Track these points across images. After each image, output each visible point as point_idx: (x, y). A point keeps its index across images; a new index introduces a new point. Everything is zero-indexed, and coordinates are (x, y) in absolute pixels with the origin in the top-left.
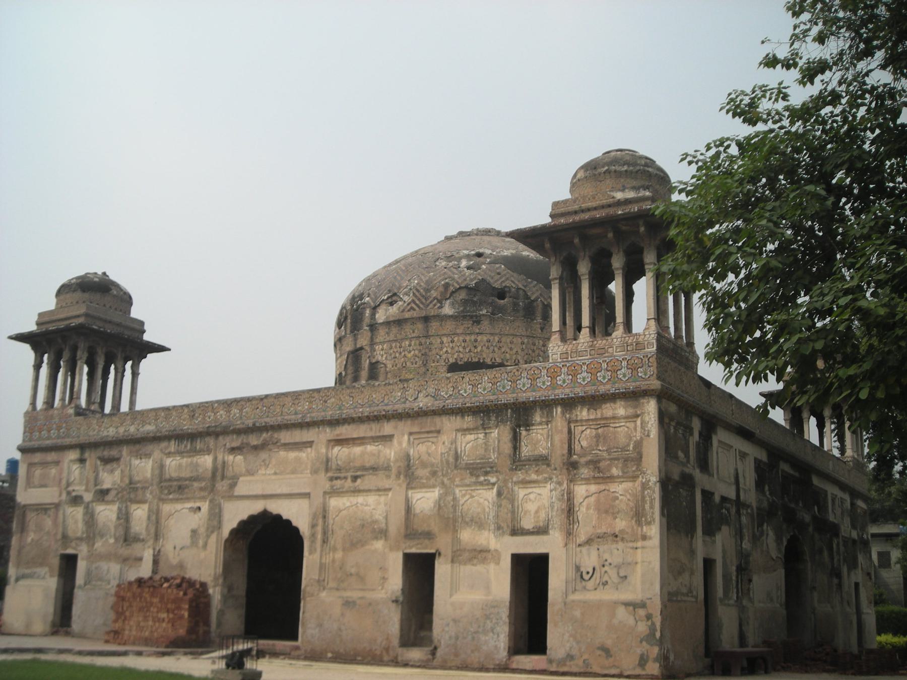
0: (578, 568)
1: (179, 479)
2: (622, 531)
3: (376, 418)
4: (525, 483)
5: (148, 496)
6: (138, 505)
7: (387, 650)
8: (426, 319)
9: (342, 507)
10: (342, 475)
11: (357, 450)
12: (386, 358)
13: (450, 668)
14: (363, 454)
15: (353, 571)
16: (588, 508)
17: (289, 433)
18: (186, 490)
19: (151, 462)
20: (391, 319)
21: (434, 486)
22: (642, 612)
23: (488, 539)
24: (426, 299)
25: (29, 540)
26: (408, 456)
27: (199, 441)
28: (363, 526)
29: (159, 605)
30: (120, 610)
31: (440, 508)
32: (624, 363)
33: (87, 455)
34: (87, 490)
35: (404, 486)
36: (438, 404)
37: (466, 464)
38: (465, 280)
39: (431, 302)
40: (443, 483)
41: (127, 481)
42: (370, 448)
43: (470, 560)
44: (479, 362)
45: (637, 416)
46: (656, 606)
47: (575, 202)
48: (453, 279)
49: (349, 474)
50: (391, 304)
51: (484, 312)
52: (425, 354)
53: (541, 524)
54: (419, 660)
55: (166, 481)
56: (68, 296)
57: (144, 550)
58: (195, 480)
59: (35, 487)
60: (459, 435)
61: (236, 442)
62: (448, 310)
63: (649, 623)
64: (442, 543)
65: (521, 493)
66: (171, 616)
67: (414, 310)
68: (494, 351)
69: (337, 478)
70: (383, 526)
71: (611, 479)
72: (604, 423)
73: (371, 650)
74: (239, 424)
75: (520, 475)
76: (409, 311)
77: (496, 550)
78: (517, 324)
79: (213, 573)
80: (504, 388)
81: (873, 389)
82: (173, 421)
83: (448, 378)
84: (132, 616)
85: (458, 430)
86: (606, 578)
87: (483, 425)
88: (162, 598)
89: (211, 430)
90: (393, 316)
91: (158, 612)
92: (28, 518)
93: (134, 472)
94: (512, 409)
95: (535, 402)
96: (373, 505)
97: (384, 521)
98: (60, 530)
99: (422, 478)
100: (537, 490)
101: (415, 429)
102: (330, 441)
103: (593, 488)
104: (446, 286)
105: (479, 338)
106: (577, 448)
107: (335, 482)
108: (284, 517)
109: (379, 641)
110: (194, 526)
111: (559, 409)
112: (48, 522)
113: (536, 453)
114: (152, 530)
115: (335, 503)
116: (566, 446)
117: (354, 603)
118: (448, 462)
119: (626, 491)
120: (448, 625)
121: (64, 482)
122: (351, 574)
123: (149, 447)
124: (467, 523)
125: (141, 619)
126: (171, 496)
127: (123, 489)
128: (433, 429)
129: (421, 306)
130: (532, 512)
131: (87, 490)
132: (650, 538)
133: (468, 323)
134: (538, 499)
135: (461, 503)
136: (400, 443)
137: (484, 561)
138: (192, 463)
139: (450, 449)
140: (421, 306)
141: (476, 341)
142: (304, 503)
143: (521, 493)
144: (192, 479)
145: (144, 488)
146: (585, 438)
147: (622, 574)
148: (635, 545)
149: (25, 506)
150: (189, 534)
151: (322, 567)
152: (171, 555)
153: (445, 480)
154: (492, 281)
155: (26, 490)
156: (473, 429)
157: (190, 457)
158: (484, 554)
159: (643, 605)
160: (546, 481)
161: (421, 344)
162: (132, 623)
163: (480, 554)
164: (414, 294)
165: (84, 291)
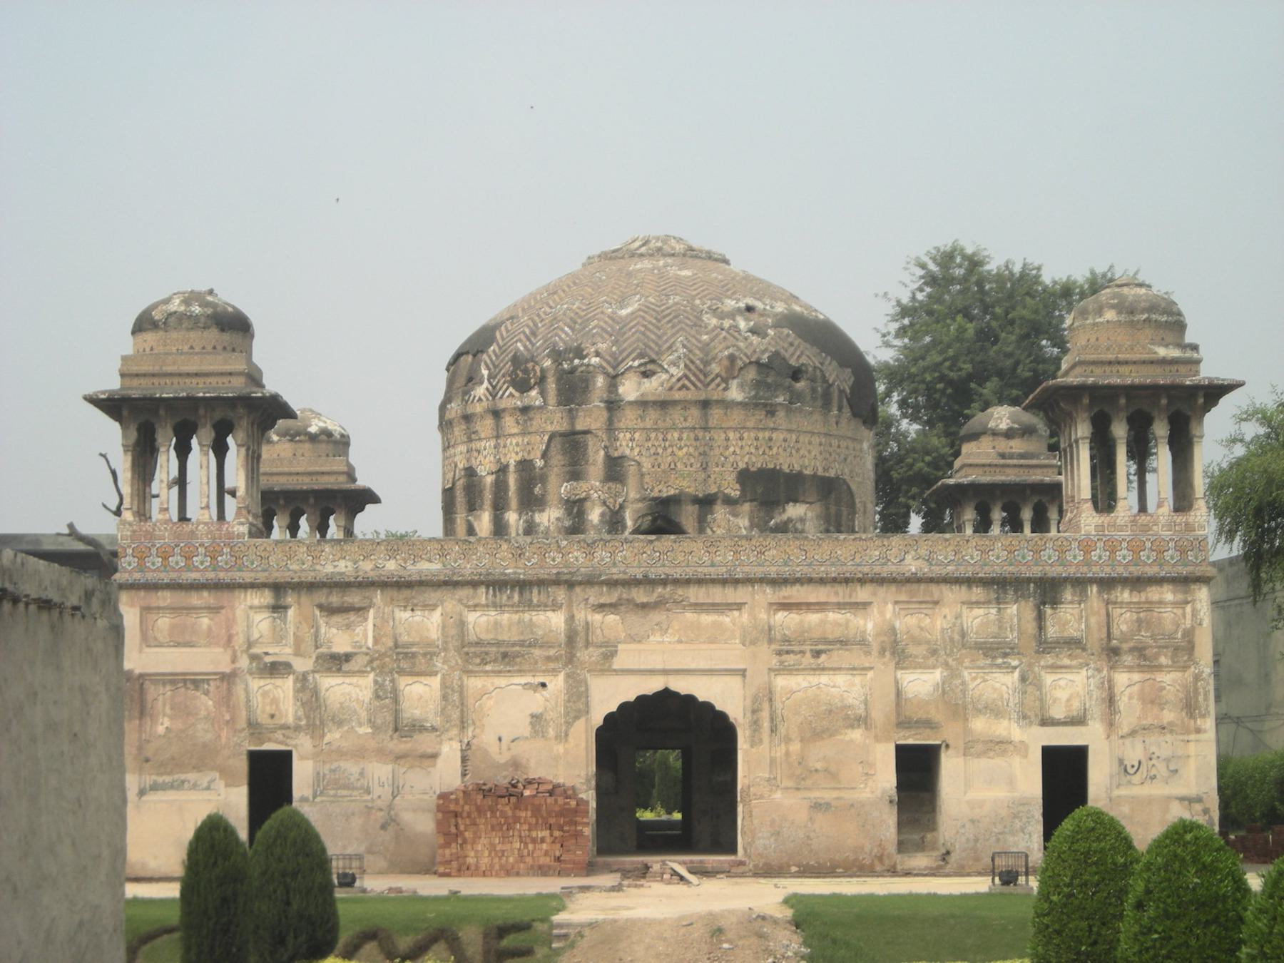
0: (1121, 762)
1: (498, 644)
2: (1171, 724)
3: (847, 581)
4: (1055, 668)
5: (439, 665)
6: (415, 679)
7: (881, 859)
8: (705, 405)
9: (795, 687)
10: (796, 648)
11: (813, 618)
12: (640, 454)
13: (969, 875)
14: (823, 622)
15: (819, 766)
16: (1130, 698)
17: (703, 589)
18: (518, 660)
19: (436, 617)
20: (650, 398)
21: (934, 667)
22: (1198, 807)
23: (1010, 729)
24: (706, 376)
25: (161, 729)
26: (893, 630)
27: (535, 591)
28: (831, 711)
29: (533, 821)
30: (453, 830)
31: (944, 692)
32: (1172, 544)
33: (290, 599)
34: (297, 653)
35: (892, 664)
36: (937, 571)
37: (976, 643)
38: (755, 351)
39: (713, 380)
40: (947, 664)
41: (391, 644)
42: (832, 616)
43: (983, 754)
44: (774, 469)
45: (1188, 603)
46: (1213, 802)
47: (1108, 349)
48: (739, 349)
49: (807, 648)
50: (646, 375)
51: (780, 399)
52: (704, 454)
53: (1075, 713)
54: (926, 868)
55: (471, 644)
56: (192, 334)
57: (441, 743)
58: (530, 646)
59: (161, 646)
60: (964, 607)
61: (613, 596)
62: (735, 393)
63: (1207, 817)
64: (948, 733)
65: (1048, 679)
66: (557, 833)
67: (688, 389)
68: (791, 455)
69: (788, 652)
70: (861, 712)
71: (1159, 668)
72: (1150, 605)
73: (856, 860)
74: (616, 574)
75: (1049, 659)
76: (680, 389)
77: (1022, 742)
78: (817, 416)
79: (583, 773)
80: (1024, 558)
81: (1272, 546)
82: (479, 559)
83: (947, 540)
84: (477, 837)
85: (963, 603)
86: (1153, 772)
87: (997, 599)
88: (536, 811)
89: (566, 577)
90: (653, 394)
91: (530, 830)
92: (149, 698)
93: (401, 630)
94: (1035, 583)
95: (1066, 580)
96: (842, 686)
97: (862, 706)
98: (244, 713)
99: (916, 657)
100: (1069, 676)
101: (903, 597)
102: (771, 604)
103: (1137, 677)
104: (732, 358)
105: (774, 436)
106: (1116, 632)
107: (785, 657)
108: (701, 700)
109: (867, 849)
110: (537, 710)
111: (1095, 588)
112: (205, 703)
113: (1066, 634)
114: (455, 715)
115: (781, 682)
116: (1105, 630)
117: (828, 805)
118: (952, 639)
119: (1174, 681)
120: (964, 826)
121: (239, 641)
122: (816, 770)
123: (432, 596)
124: (979, 711)
125: (497, 841)
126: (488, 668)
127: (382, 656)
128: (928, 599)
129: (699, 384)
130: (1064, 700)
131: (297, 653)
132: (1205, 731)
133: (760, 414)
134: (1069, 686)
135: (971, 687)
136: (882, 613)
137: (1004, 753)
138: (519, 622)
139: (954, 624)
140: (699, 384)
141: (770, 439)
142: (736, 682)
143: (1048, 679)
144: (521, 643)
145: (429, 655)
146: (1124, 621)
147: (1172, 768)
148: (1186, 738)
149: (141, 676)
150: (529, 720)
151: (773, 761)
152: (493, 749)
153: (950, 660)
154: (787, 356)
155: (141, 651)
156: (984, 603)
157: (517, 612)
158: (1003, 746)
159: (1199, 800)
160: (1081, 666)
161: (697, 439)
162: (479, 847)
163: (999, 746)
164: (686, 366)
165: (223, 330)
